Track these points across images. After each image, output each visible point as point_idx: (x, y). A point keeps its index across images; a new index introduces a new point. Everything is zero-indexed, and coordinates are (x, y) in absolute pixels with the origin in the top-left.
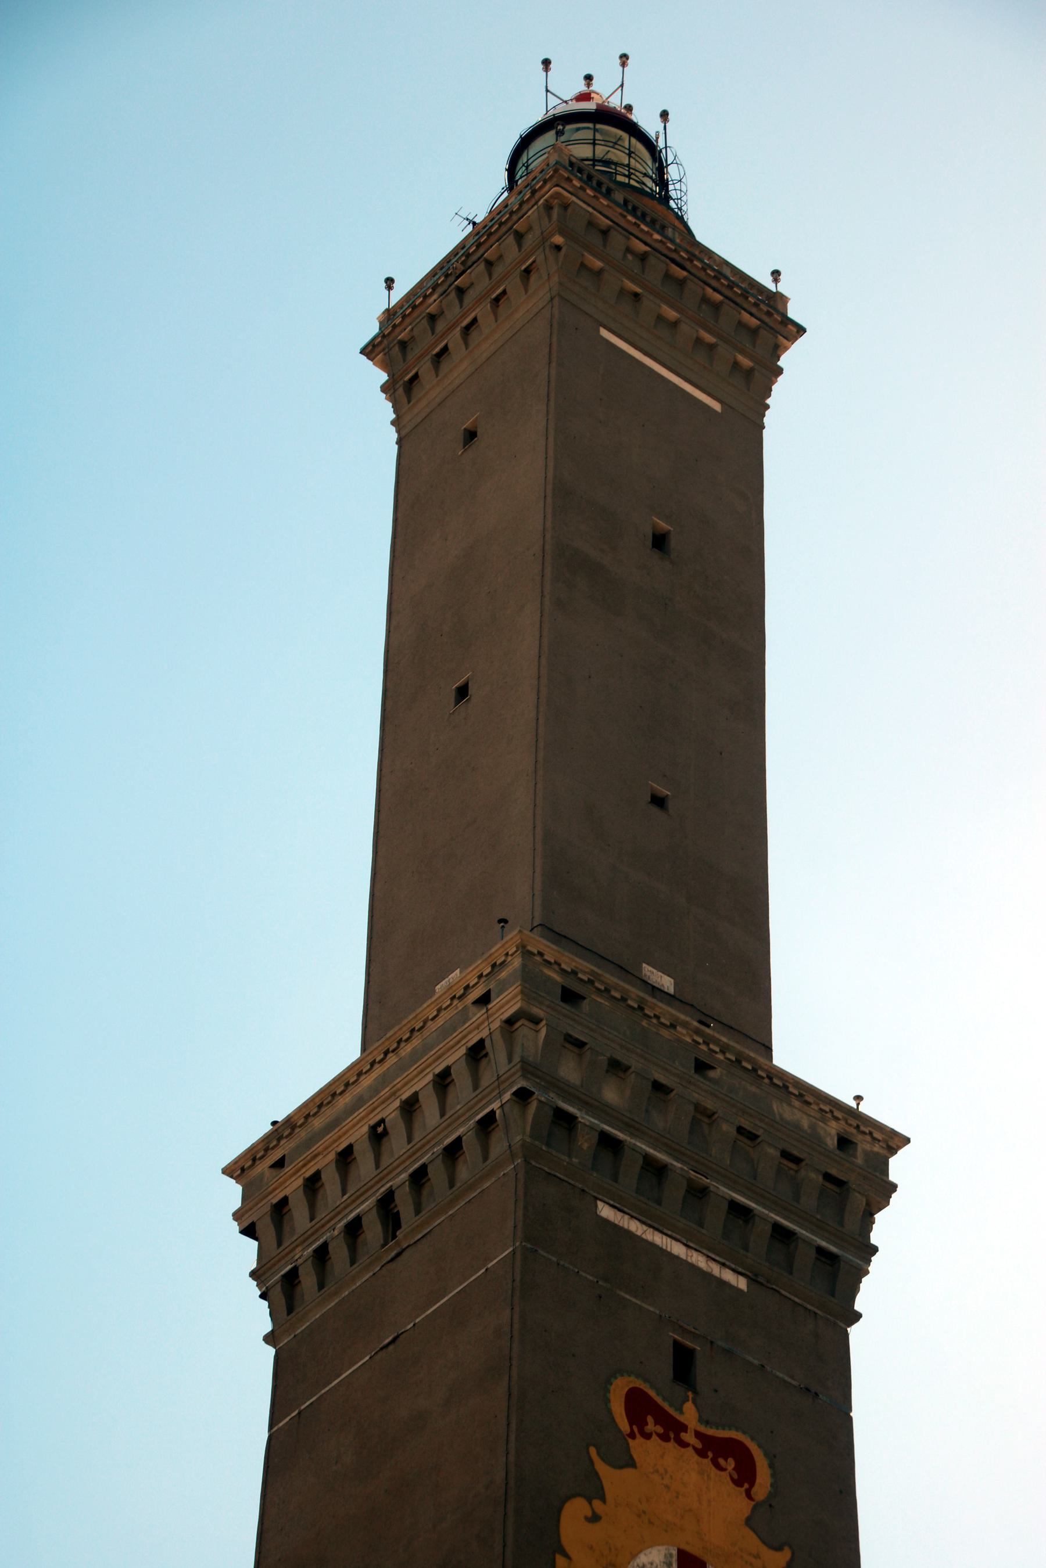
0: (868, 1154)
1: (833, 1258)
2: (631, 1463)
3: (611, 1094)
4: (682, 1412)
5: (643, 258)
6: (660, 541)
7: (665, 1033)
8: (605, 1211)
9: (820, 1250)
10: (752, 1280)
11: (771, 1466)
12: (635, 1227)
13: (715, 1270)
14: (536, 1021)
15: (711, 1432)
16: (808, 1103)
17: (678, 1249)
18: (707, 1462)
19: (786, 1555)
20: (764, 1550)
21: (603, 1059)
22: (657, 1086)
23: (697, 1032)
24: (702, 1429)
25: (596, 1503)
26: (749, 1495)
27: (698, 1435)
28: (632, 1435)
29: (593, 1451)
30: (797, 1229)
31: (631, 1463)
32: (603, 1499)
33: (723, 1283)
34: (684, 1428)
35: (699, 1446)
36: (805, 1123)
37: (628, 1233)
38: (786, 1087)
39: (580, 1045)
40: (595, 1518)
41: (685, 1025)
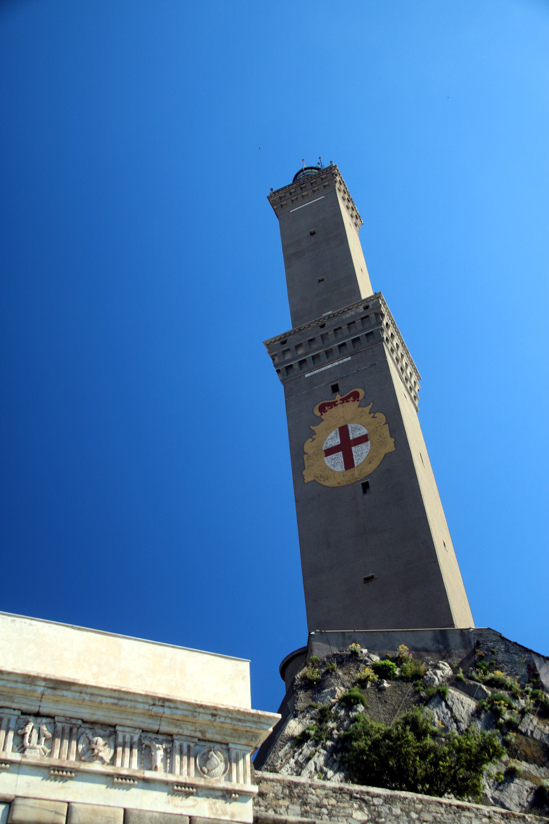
0: (372, 305)
1: (372, 332)
2: (323, 420)
3: (301, 351)
4: (335, 399)
5: (295, 191)
6: (312, 234)
7: (309, 328)
8: (307, 375)
9: (367, 335)
10: (352, 355)
11: (364, 389)
12: (316, 372)
13: (341, 362)
14: (276, 355)
15: (344, 396)
16: (352, 309)
17: (330, 366)
18: (345, 404)
19: (372, 404)
20: (364, 408)
21: (294, 348)
22: (311, 340)
23: (315, 321)
24: (342, 397)
25: (314, 437)
26: (358, 401)
27: (340, 400)
28: (322, 414)
29: (311, 427)
30: (358, 336)
31: (323, 420)
32: (316, 434)
33: (343, 363)
34: (337, 401)
35: (341, 402)
36: (353, 313)
37: (315, 374)
38: (344, 311)
39: (288, 350)
40: (314, 439)
41: (312, 323)
